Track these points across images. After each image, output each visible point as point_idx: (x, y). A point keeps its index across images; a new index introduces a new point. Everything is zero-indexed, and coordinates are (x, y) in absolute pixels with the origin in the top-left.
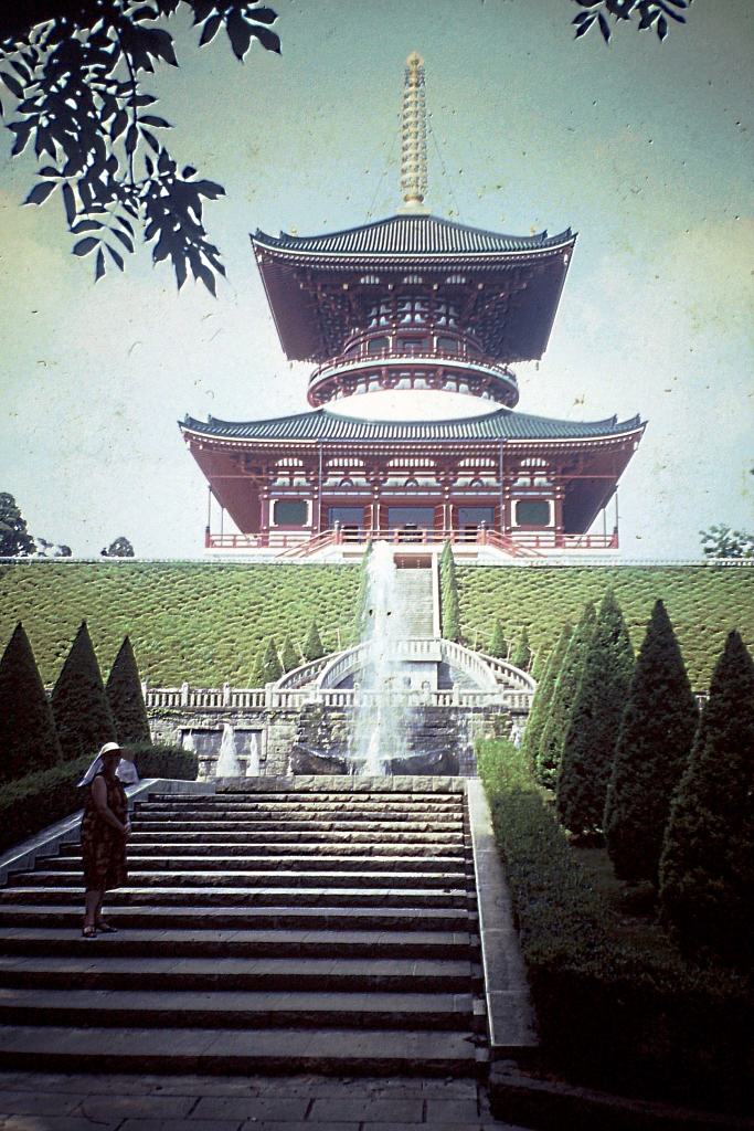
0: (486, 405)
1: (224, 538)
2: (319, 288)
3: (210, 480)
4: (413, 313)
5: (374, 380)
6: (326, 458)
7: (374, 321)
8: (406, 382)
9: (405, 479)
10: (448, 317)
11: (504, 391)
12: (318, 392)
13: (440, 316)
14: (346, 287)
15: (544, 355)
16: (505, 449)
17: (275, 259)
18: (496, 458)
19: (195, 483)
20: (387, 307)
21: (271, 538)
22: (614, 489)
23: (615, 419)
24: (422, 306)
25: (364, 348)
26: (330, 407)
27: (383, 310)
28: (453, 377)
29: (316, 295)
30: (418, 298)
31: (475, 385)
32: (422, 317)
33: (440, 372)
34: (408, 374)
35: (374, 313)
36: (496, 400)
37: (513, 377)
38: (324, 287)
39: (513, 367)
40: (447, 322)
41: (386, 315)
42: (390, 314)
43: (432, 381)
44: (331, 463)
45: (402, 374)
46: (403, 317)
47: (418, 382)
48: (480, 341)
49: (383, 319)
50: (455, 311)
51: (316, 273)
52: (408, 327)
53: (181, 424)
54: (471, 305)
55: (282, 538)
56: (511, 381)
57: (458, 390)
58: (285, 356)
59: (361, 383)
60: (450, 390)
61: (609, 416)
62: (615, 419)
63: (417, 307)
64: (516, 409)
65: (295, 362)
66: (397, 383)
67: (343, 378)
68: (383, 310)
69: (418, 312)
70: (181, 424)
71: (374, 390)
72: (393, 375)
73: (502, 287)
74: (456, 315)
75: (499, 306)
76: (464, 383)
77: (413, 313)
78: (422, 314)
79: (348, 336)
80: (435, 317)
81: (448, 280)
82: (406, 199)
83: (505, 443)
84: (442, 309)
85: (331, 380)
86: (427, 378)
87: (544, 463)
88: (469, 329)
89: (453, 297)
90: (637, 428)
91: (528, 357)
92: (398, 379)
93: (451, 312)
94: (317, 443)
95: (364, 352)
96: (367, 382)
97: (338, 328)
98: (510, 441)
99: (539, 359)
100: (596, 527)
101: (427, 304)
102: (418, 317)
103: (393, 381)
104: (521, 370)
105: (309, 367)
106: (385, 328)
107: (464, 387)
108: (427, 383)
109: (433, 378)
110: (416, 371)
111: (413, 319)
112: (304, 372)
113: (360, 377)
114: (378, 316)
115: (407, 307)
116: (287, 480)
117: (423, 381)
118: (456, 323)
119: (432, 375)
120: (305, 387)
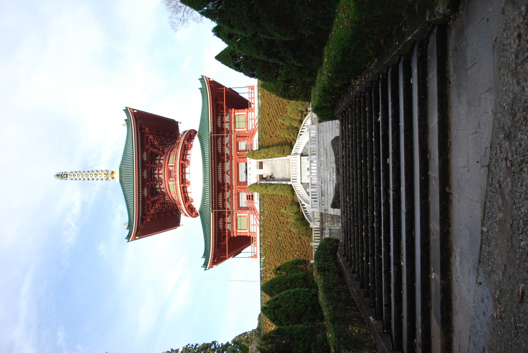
0: (196, 142)
1: (253, 251)
2: (149, 213)
3: (229, 257)
4: (159, 174)
6: (219, 208)
7: (162, 190)
9: (227, 176)
10: (160, 159)
11: (190, 135)
12: (192, 213)
13: (160, 163)
14: (148, 202)
15: (176, 120)
16: (214, 133)
17: (137, 231)
18: (218, 137)
19: (230, 263)
20: (157, 185)
21: (252, 231)
22: (230, 89)
23: (200, 89)
24: (156, 170)
25: (173, 194)
26: (197, 209)
27: (158, 186)
28: (185, 156)
29: (152, 215)
30: (152, 172)
31: (188, 147)
32: (160, 170)
33: (182, 162)
34: (184, 175)
35: (159, 190)
36: (194, 138)
37: (185, 132)
38: (148, 211)
39: (181, 131)
40: (163, 160)
42: (159, 184)
44: (221, 207)
48: (170, 146)
49: (162, 187)
50: (158, 156)
51: (144, 214)
53: (205, 270)
54: (155, 150)
55: (252, 226)
56: (186, 133)
57: (190, 154)
58: (178, 228)
60: (190, 157)
61: (199, 91)
62: (200, 89)
63: (156, 172)
64: (197, 131)
65: (181, 223)
67: (186, 203)
68: (158, 186)
69: (158, 172)
70: (205, 270)
72: (184, 181)
73: (147, 137)
74: (159, 156)
75: (156, 138)
77: (159, 174)
78: (159, 170)
79: (169, 201)
80: (160, 165)
81: (145, 159)
82: (113, 178)
83: (211, 133)
84: (157, 162)
85: (186, 208)
86: (185, 167)
87: (220, 118)
88: (165, 151)
89: (153, 157)
90: (204, 79)
91: (177, 127)
93: (158, 158)
94: (212, 212)
95: (175, 194)
97: (166, 205)
98: (210, 132)
99: (177, 122)
100: (246, 96)
101: (155, 168)
104: (182, 128)
105: (183, 218)
107: (189, 152)
109: (185, 165)
112: (185, 219)
113: (185, 195)
115: (156, 176)
116: (229, 225)
118: (163, 156)
119: (184, 166)
120: (190, 219)
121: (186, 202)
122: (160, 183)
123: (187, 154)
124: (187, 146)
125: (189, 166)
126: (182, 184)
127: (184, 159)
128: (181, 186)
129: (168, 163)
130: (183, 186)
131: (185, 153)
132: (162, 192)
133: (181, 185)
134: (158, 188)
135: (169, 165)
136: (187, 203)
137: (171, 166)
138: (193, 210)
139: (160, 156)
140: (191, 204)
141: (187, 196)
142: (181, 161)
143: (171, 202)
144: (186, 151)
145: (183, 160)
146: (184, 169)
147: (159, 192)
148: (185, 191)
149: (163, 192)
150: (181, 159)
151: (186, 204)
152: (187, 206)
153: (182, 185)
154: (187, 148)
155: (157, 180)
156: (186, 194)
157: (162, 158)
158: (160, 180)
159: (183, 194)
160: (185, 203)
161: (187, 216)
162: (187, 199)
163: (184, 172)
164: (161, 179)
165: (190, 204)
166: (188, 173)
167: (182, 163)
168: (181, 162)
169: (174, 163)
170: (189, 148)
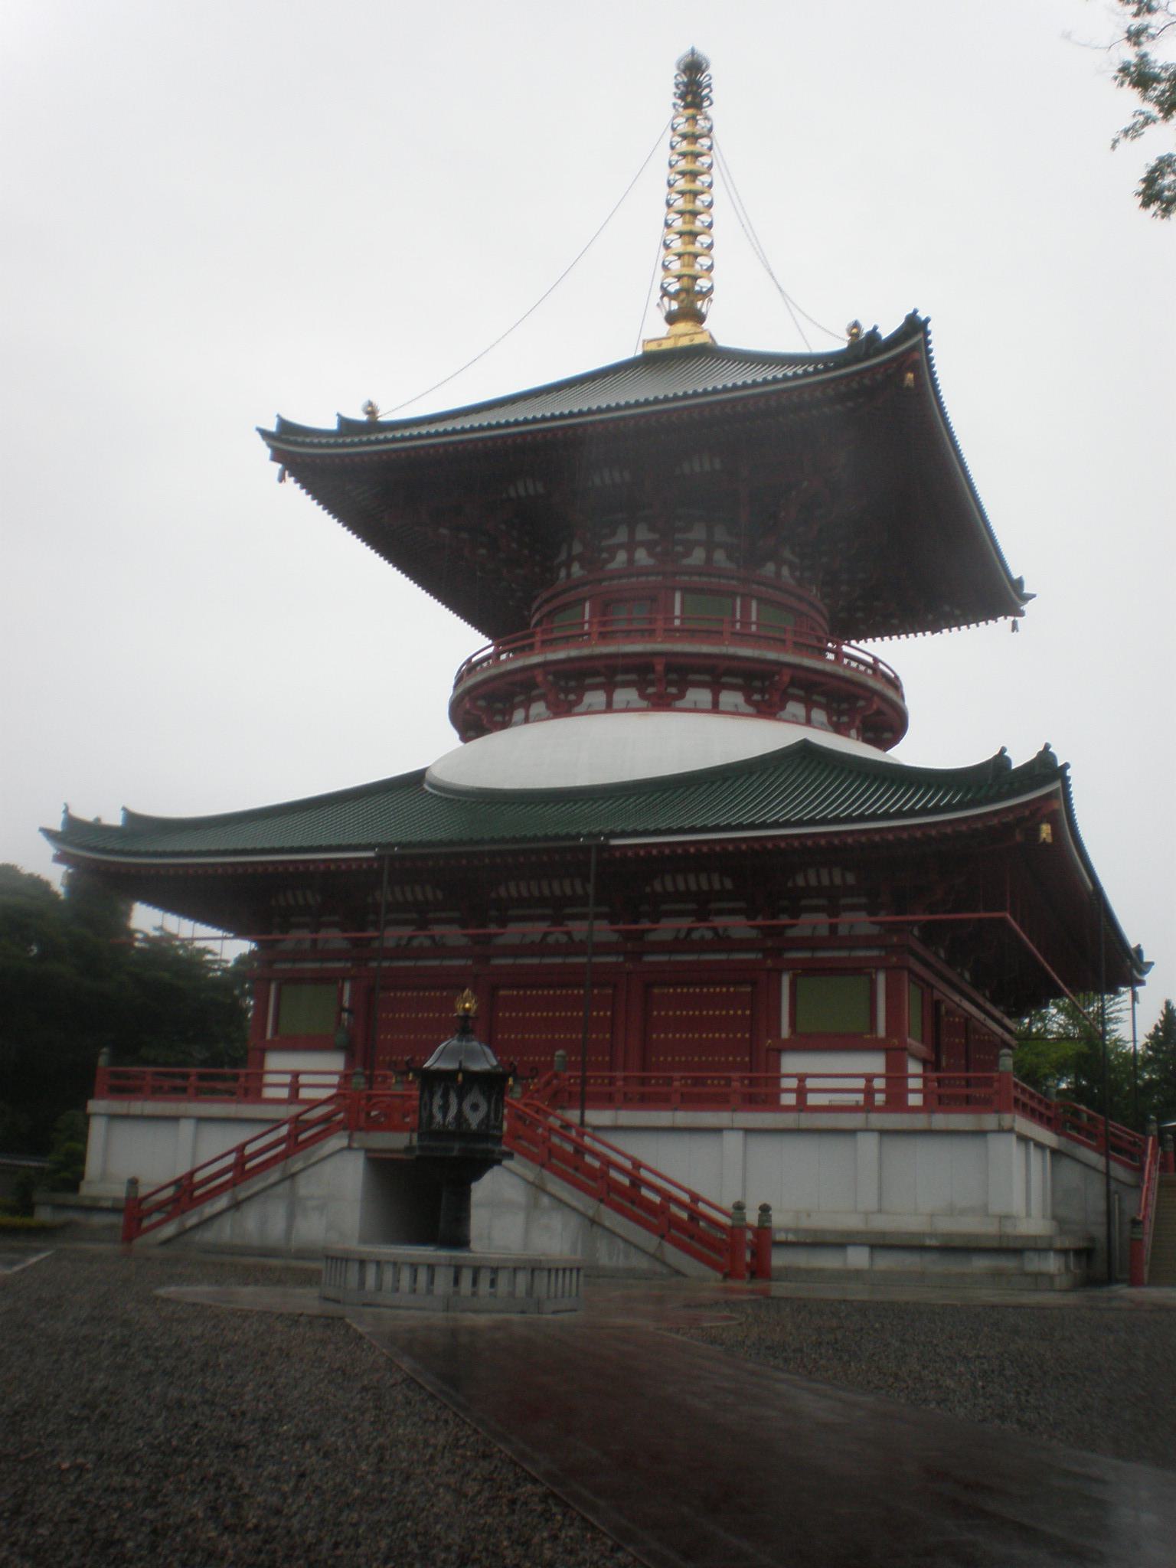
5: (626, 684)
7: (622, 557)
8: (703, 696)
27: (642, 533)
28: (801, 693)
31: (840, 713)
32: (730, 557)
35: (622, 536)
41: (650, 546)
43: (757, 697)
46: (687, 554)
47: (729, 698)
52: (700, 574)
63: (720, 534)
66: (681, 695)
71: (627, 709)
72: (673, 676)
76: (819, 706)
77: (710, 546)
86: (747, 691)
92: (683, 686)
96: (609, 688)
102: (719, 556)
103: (673, 690)
106: (645, 572)
109: (762, 691)
110: (729, 672)
111: (709, 559)
113: (596, 673)
114: (631, 547)
115: (698, 533)
119: (757, 684)
122: (658, 549)
123: (809, 705)
124: (844, 706)
129: (762, 601)
130: (659, 668)
131: (816, 698)
132: (612, 551)
134: (632, 533)
135: (754, 605)
136: (550, 678)
138: (499, 706)
139: (797, 560)
144: (823, 700)
145: (793, 683)
147: (613, 534)
149: (612, 558)
154: (835, 705)
155: (678, 536)
157: (785, 571)
158: (679, 549)
162: (573, 684)
165: (535, 692)
166: (695, 703)
170: (835, 719)
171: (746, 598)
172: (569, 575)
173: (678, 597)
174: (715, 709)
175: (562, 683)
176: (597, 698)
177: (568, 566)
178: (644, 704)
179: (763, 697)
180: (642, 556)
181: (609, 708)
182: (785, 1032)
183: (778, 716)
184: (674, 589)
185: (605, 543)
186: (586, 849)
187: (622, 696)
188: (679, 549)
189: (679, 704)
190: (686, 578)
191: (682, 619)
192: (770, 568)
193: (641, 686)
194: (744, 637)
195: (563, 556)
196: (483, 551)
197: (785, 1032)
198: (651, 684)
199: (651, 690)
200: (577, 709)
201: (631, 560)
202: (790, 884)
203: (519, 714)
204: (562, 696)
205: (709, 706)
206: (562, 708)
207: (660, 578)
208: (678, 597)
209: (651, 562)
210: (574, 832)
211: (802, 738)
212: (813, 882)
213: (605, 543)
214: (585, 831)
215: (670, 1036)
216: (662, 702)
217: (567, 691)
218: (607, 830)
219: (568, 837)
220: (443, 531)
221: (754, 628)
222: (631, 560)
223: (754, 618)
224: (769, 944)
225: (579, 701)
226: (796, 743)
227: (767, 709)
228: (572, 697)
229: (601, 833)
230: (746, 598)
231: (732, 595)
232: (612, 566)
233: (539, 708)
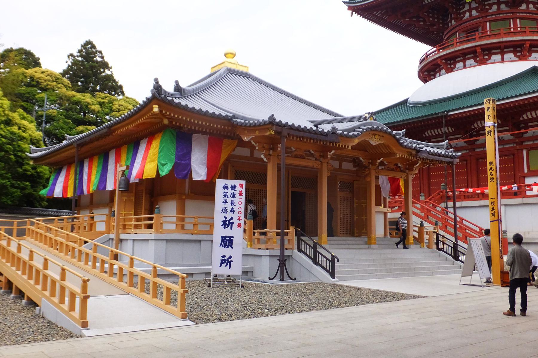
7: (467, 14)
8: (498, 57)
32: (507, 6)
33: (528, 45)
34: (499, 51)
41: (476, 9)
43: (519, 54)
45: (493, 51)
46: (491, 8)
47: (507, 56)
52: (495, 15)
59: (459, 61)
66: (490, 58)
67: (445, 59)
71: (471, 66)
72: (486, 52)
92: (490, 55)
96: (464, 61)
103: (486, 57)
106: (476, 18)
108: (516, 56)
109: (521, 51)
111: (499, 8)
113: (459, 57)
114: (470, 11)
117: (511, 55)
118: (534, 7)
121: (446, 60)
125: (517, 59)
126: (481, 49)
127: (533, 49)
128: (477, 48)
129: (521, 19)
132: (464, 13)
133: (479, 48)
135: (518, 20)
136: (443, 61)
137: (515, 24)
138: (432, 73)
140: (443, 68)
141: (457, 60)
142: (529, 42)
143: (445, 33)
145: (531, 46)
146: (512, 49)
147: (464, 7)
148: (467, 57)
149: (464, 16)
150: (533, 42)
151: (442, 60)
152: (439, 62)
153: (479, 50)
156: (461, 58)
157: (531, 6)
158: (487, 7)
159: (461, 54)
160: (443, 58)
161: (420, 63)
162: (452, 62)
163: (506, 50)
164: (488, 10)
165: (441, 67)
167: (524, 44)
168: (527, 42)
169: (523, 30)
171: (515, 20)
172: (451, 25)
173: (488, 24)
174: (503, 60)
175: (449, 62)
176: (460, 65)
177: (451, 21)
178: (476, 64)
179: (521, 53)
180: (474, 13)
181: (465, 67)
182: (526, 171)
183: (528, 59)
184: (486, 22)
185: (461, 11)
186: (441, 117)
187: (468, 62)
188: (487, 7)
189: (489, 62)
190: (491, 17)
191: (490, 31)
192: (524, 7)
193: (475, 58)
194: (516, 33)
195: (449, 19)
196: (422, 23)
197: (526, 171)
198: (478, 57)
199: (478, 59)
200: (455, 70)
201: (471, 15)
202: (521, 119)
203: (438, 74)
204: (449, 66)
205: (500, 60)
206: (450, 70)
207: (481, 19)
208: (488, 24)
209: (477, 14)
210: (437, 112)
211: (534, 65)
212: (530, 117)
213: (461, 11)
214: (440, 111)
215: (463, 178)
216: (483, 62)
217: (450, 64)
218: (447, 110)
219: (436, 114)
220: (407, 20)
221: (519, 29)
222: (471, 15)
223: (519, 26)
224: (517, 141)
225: (455, 67)
226: (531, 68)
227: (523, 58)
228: (452, 66)
229: (446, 111)
230: (515, 20)
231: (509, 19)
232: (465, 18)
233: (443, 71)
